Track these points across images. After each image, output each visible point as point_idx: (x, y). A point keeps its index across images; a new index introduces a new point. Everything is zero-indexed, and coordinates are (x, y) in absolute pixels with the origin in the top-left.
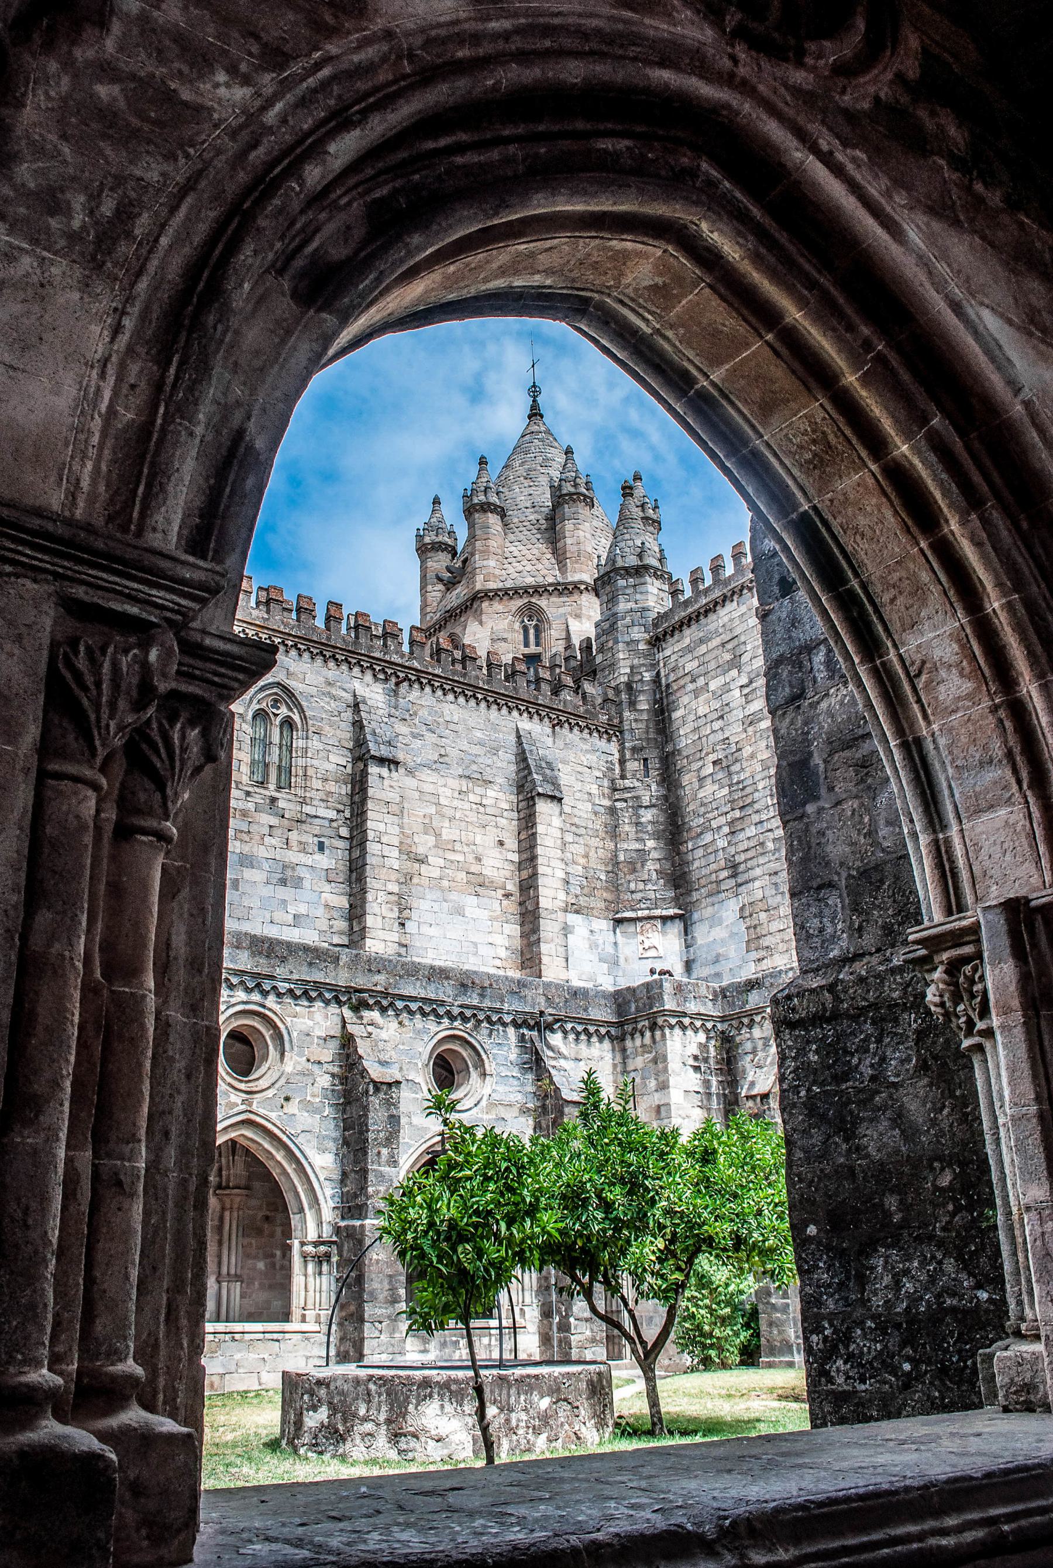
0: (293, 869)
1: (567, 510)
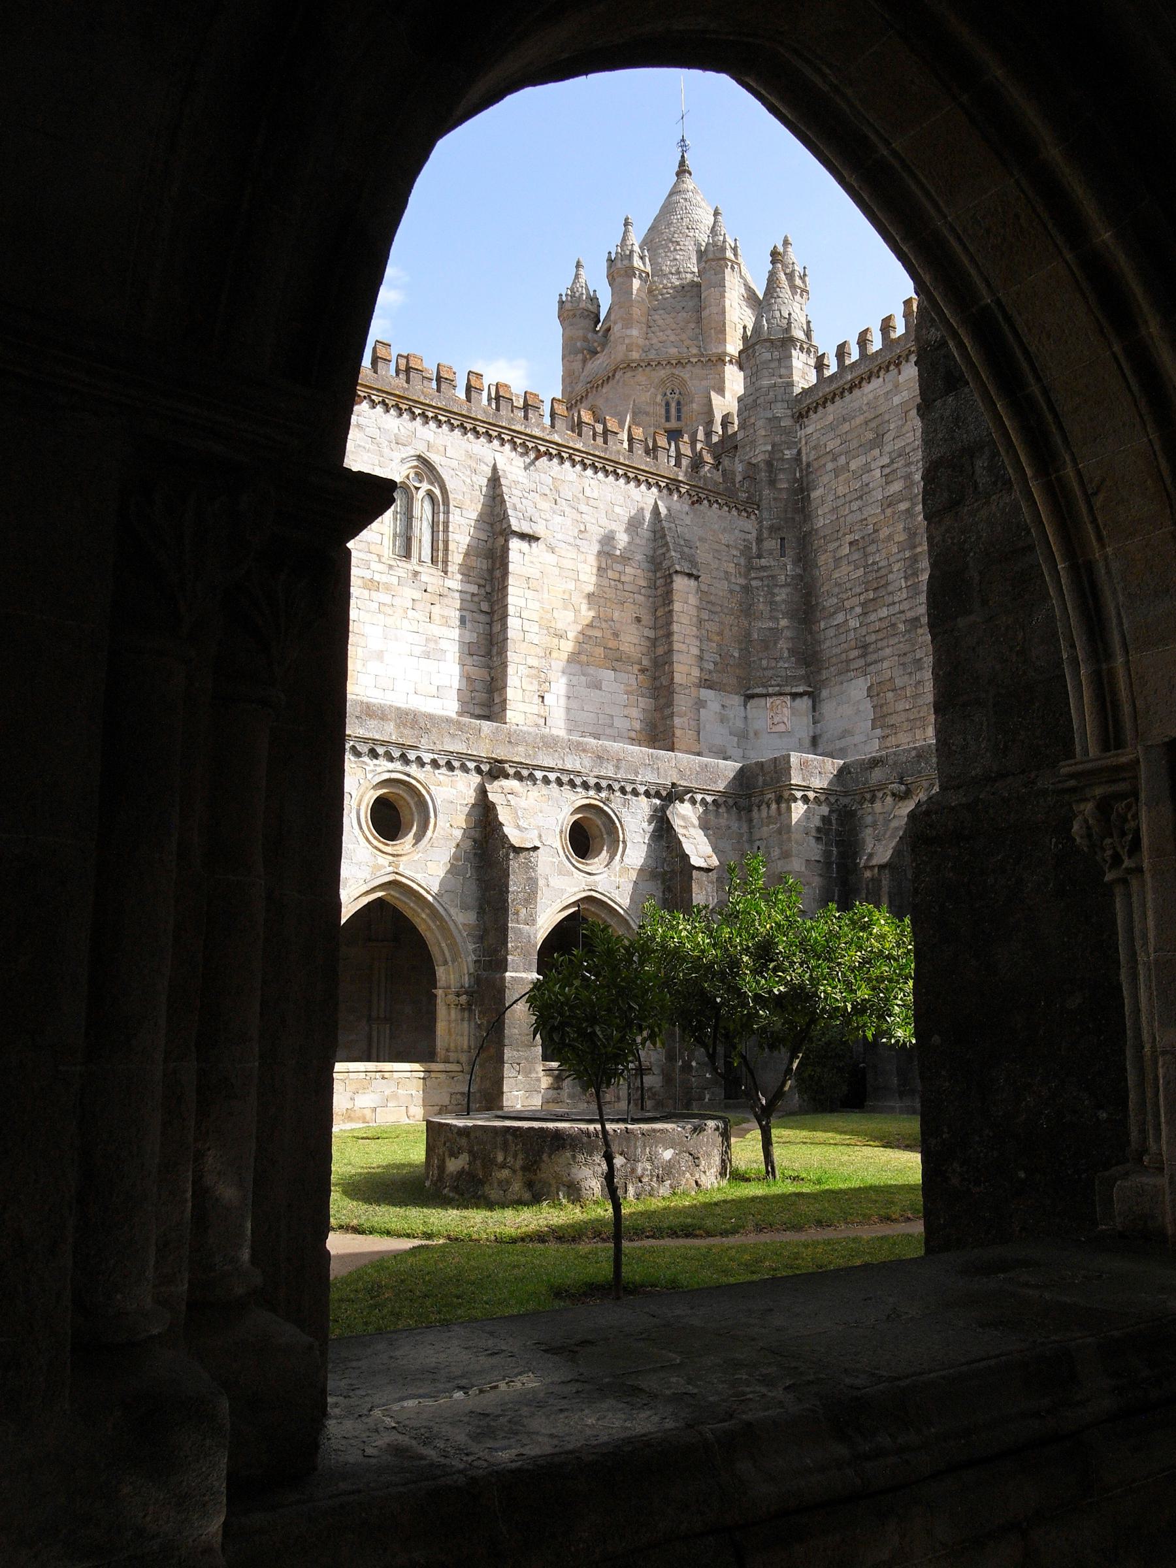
0: (436, 642)
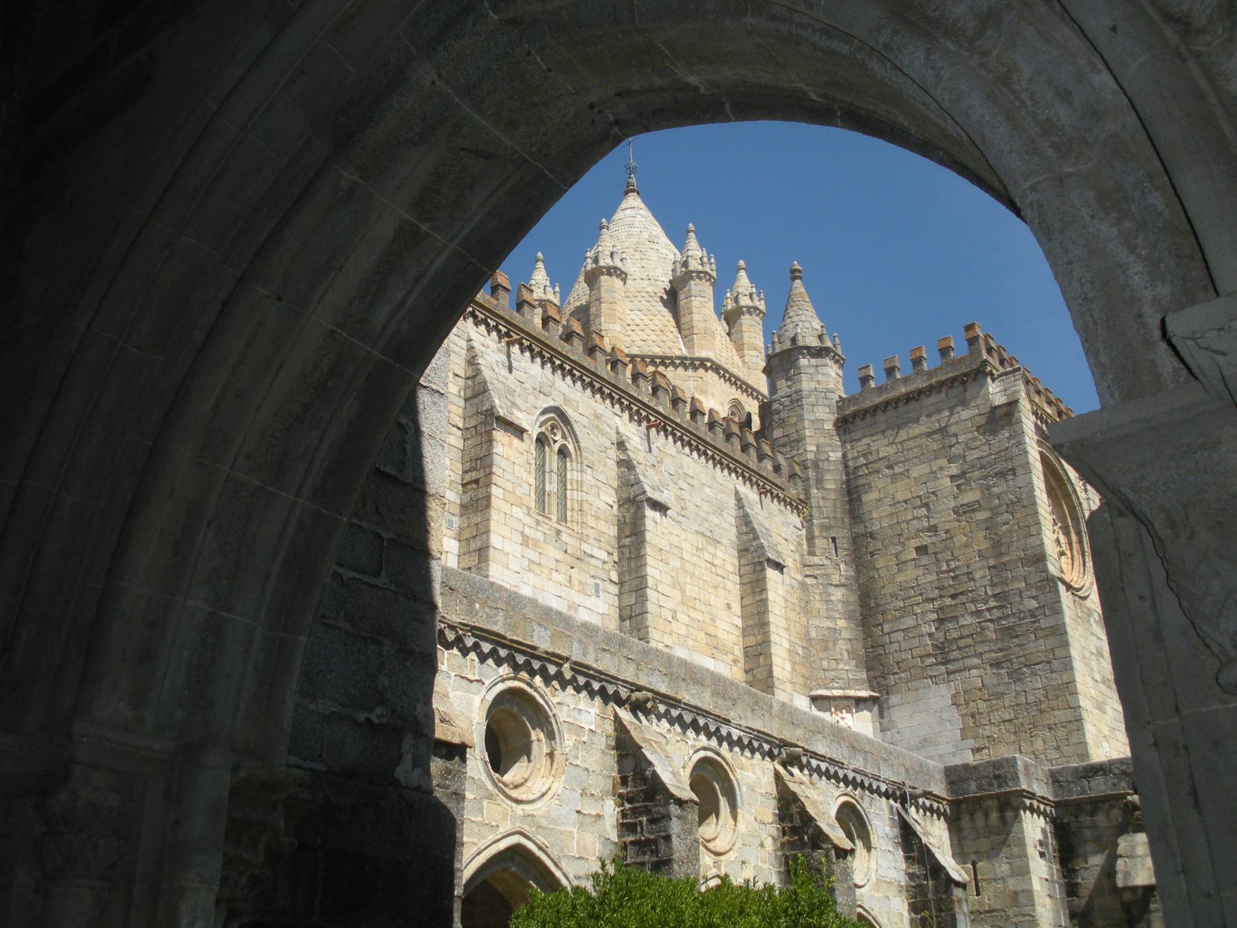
1: (693, 287)
